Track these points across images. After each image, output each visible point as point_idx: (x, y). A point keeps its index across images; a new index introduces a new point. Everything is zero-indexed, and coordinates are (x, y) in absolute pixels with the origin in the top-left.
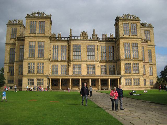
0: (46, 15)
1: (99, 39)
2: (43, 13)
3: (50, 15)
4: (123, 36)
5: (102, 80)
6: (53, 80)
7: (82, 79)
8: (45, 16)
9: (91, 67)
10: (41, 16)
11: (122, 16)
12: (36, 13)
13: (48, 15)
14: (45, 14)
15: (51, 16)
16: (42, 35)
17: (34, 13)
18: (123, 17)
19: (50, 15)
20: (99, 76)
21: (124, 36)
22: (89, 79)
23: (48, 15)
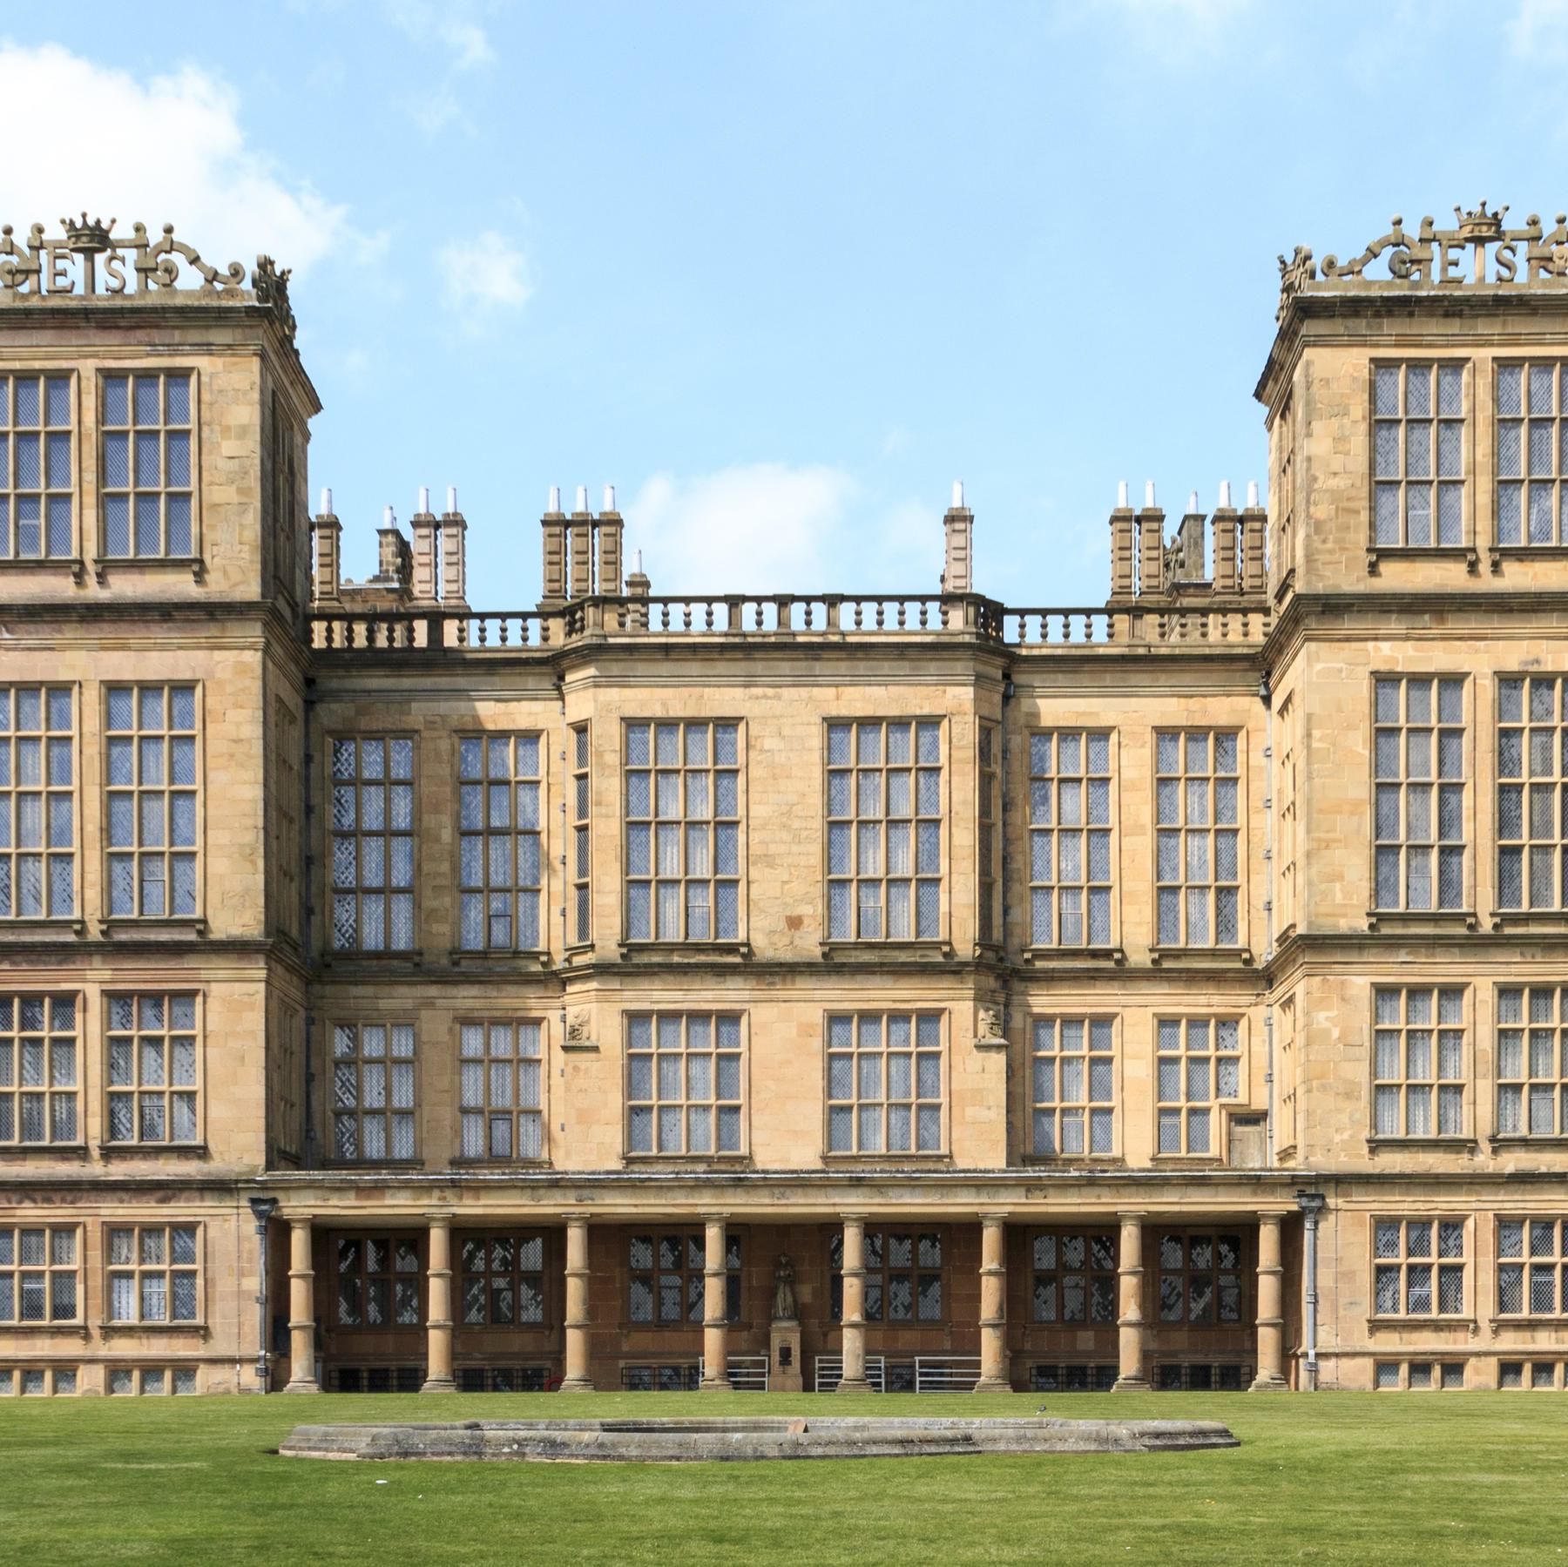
0: (213, 276)
1: (1011, 625)
2: (155, 236)
3: (265, 264)
4: (1373, 569)
5: (1018, 1233)
6: (324, 1234)
7: (738, 1233)
8: (189, 280)
9: (880, 1040)
10: (131, 288)
11: (1373, 254)
12: (57, 233)
13: (236, 272)
14: (195, 261)
15: (272, 284)
16: (179, 586)
17: (21, 239)
18: (1378, 271)
19: (265, 264)
20: (981, 1183)
21: (1386, 568)
22: (831, 1228)
23: (236, 272)
